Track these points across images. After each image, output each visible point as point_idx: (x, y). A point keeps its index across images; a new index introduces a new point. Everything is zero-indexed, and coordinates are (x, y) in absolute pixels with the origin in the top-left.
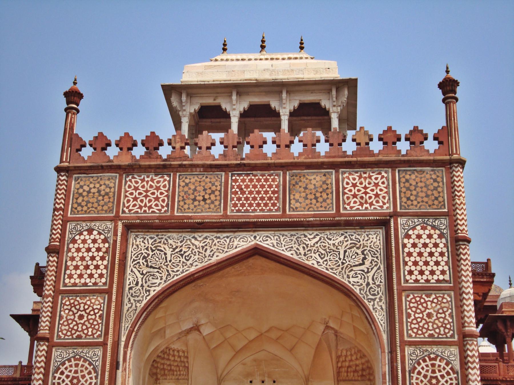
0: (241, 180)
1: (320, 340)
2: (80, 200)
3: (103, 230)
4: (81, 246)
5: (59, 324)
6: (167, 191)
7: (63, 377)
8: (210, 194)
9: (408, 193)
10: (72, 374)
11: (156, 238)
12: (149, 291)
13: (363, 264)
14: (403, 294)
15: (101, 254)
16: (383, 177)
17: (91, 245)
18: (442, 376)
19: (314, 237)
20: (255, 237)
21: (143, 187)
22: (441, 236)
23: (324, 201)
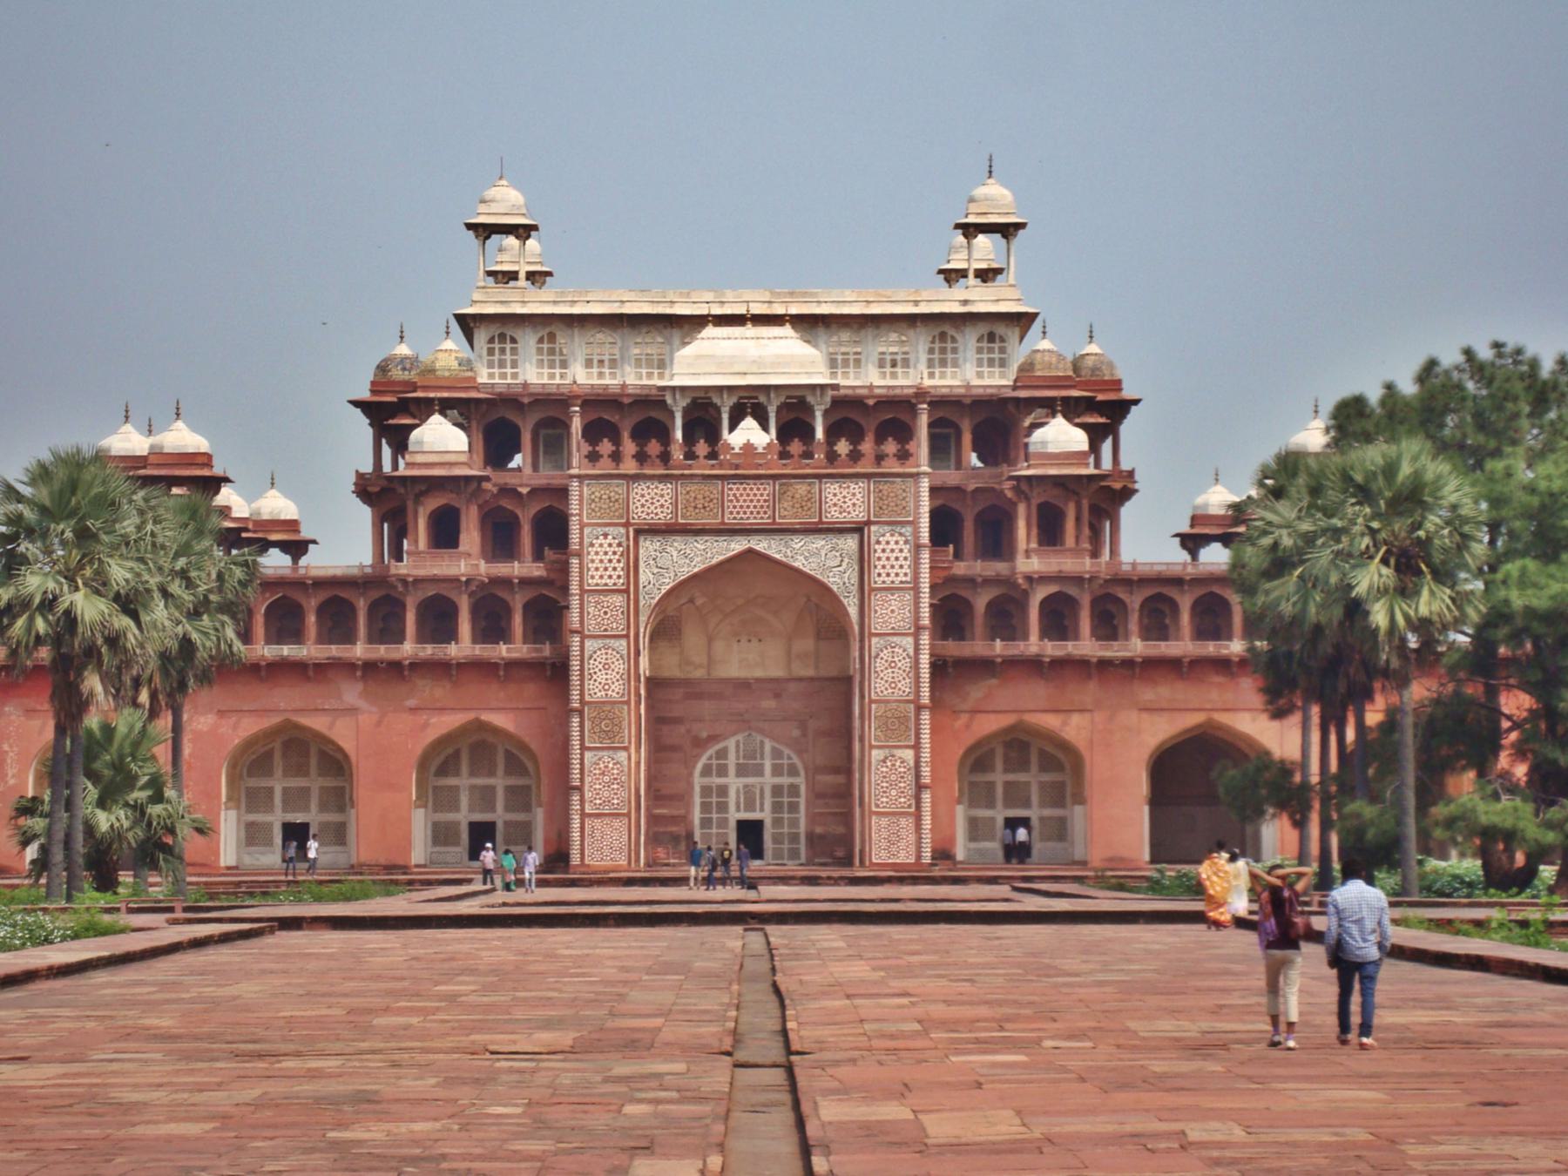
0: (734, 489)
22: (906, 542)
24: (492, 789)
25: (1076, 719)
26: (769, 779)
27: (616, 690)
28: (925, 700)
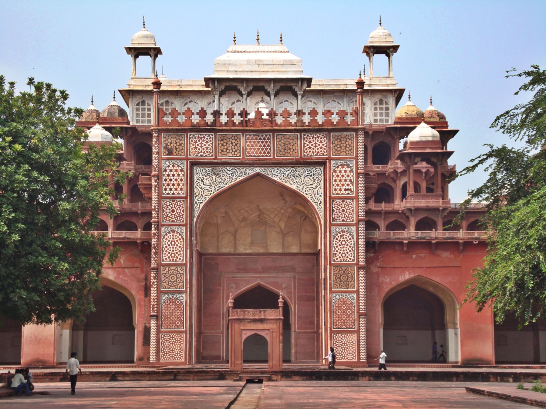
22: (351, 171)
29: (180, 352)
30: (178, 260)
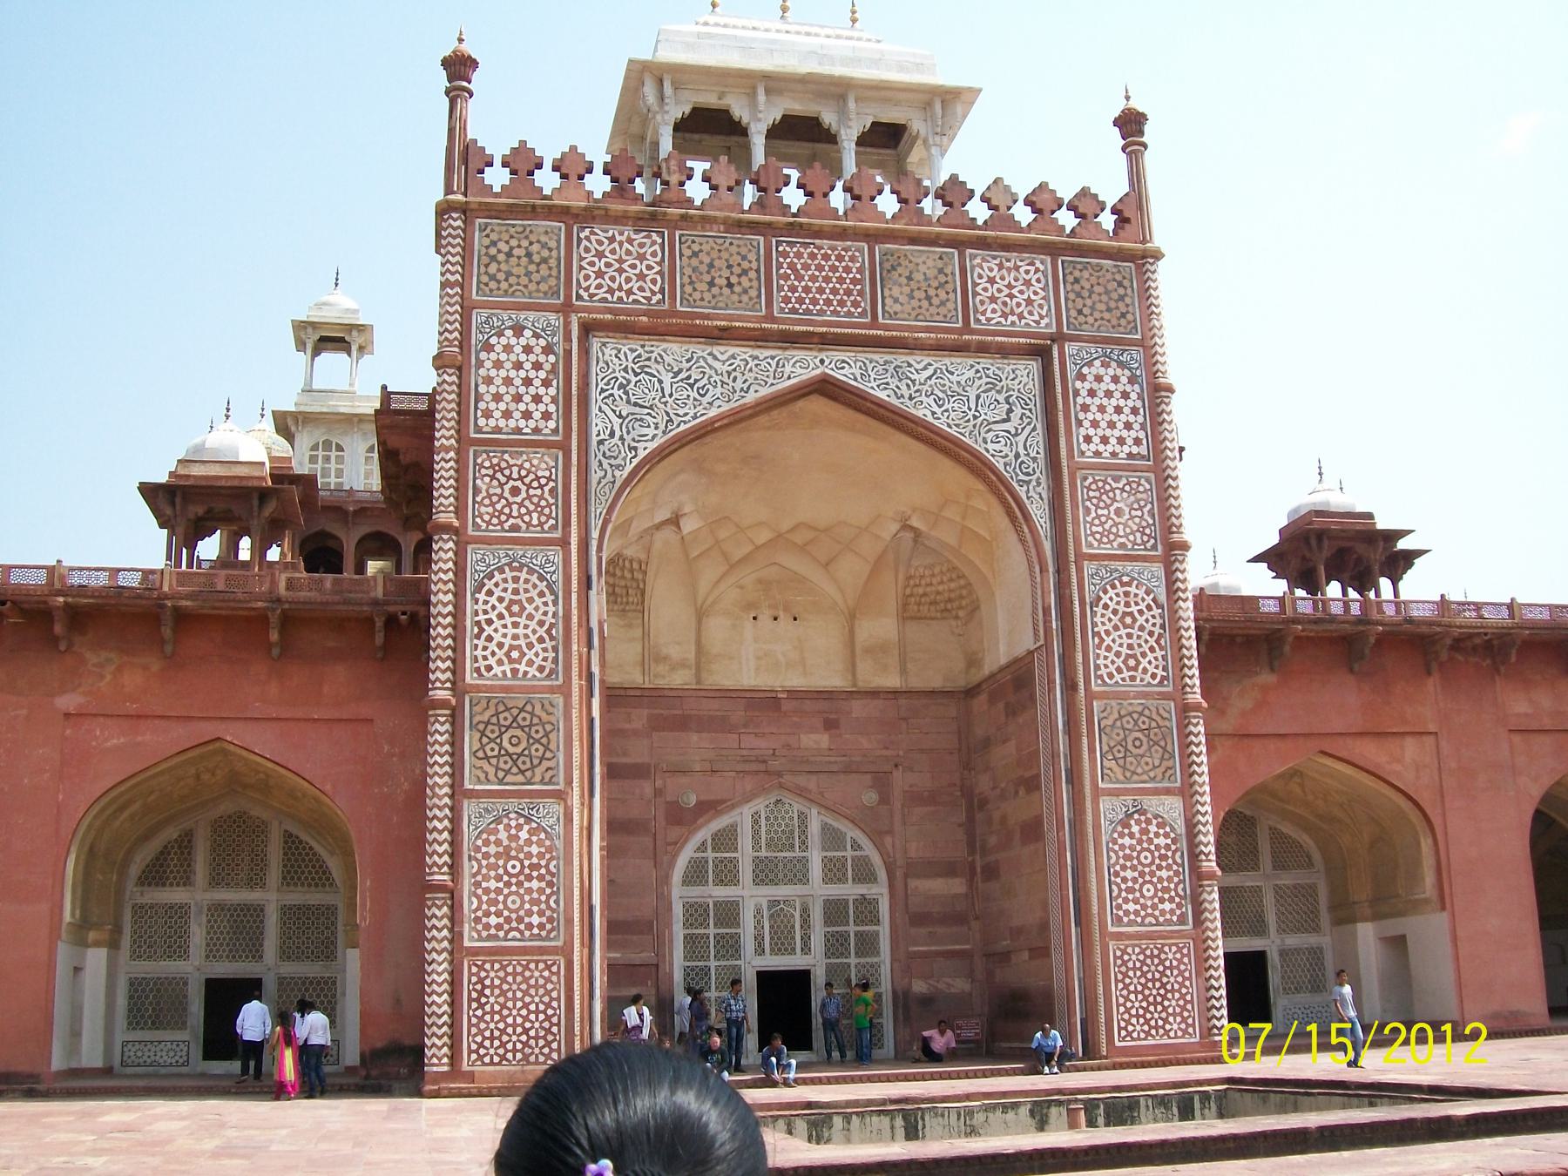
1: (884, 552)
2: (493, 268)
3: (543, 330)
4: (503, 357)
5: (474, 502)
6: (660, 264)
7: (493, 601)
8: (739, 276)
9: (1079, 302)
10: (508, 596)
11: (640, 350)
12: (635, 449)
13: (1008, 420)
14: (1079, 474)
15: (542, 375)
16: (1037, 270)
17: (523, 357)
18: (1141, 612)
19: (925, 368)
20: (822, 361)
21: (613, 252)
23: (943, 303)
24: (257, 911)
25: (1411, 749)
26: (818, 888)
27: (534, 664)
28: (1196, 697)
29: (548, 1031)
30: (533, 671)
